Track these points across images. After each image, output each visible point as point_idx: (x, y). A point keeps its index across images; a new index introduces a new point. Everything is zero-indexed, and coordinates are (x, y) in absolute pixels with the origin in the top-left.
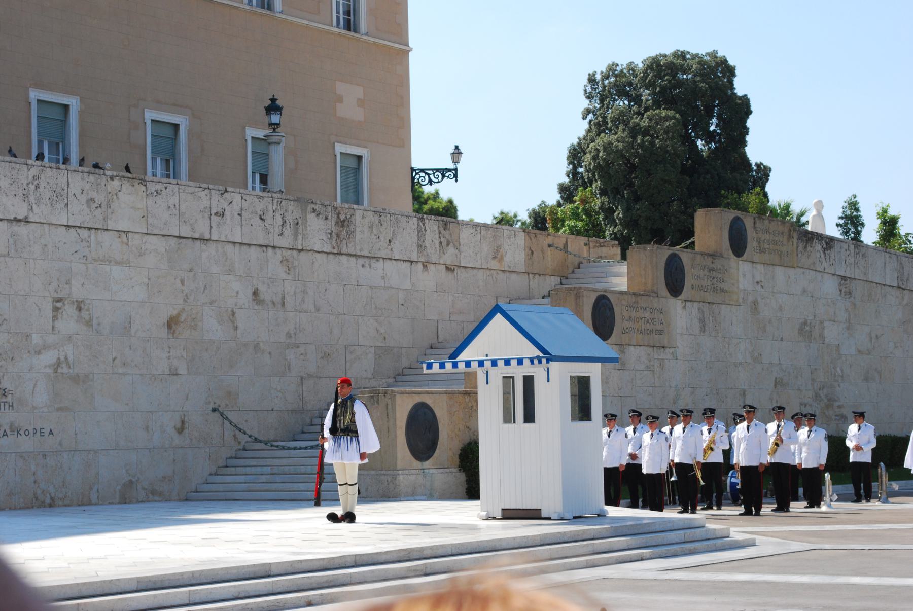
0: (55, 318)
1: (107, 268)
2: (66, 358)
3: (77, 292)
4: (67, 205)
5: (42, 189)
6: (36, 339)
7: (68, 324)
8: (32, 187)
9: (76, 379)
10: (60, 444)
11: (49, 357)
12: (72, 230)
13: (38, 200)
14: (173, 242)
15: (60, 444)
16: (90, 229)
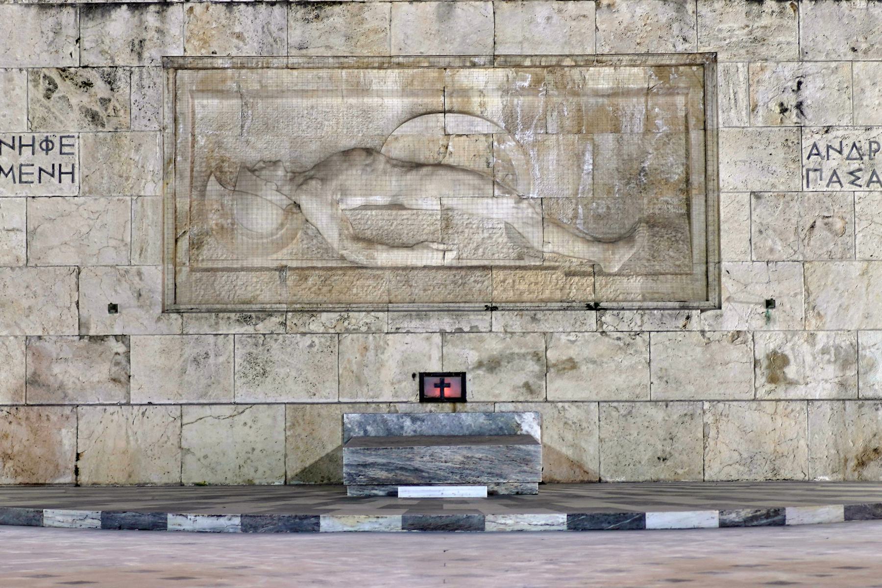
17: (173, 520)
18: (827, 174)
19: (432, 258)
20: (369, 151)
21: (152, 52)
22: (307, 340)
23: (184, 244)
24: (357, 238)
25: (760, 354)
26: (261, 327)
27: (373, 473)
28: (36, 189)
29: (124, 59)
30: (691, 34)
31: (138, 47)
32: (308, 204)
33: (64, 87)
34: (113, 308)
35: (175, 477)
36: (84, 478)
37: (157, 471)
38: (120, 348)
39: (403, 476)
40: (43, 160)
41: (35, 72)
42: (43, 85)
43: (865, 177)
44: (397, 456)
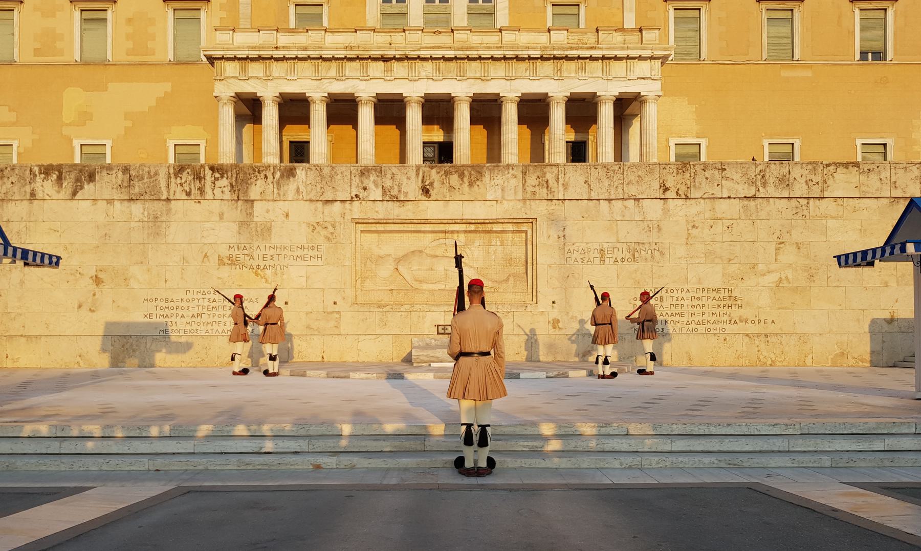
0: (777, 254)
1: (824, 221)
2: (787, 278)
3: (796, 236)
4: (788, 185)
5: (767, 177)
6: (761, 267)
7: (789, 256)
8: (759, 177)
9: (795, 290)
10: (781, 329)
11: (774, 277)
12: (794, 200)
13: (764, 185)
14: (886, 201)
15: (781, 329)
16: (808, 198)
17: (352, 375)
18: (573, 259)
19: (441, 287)
20: (420, 252)
21: (348, 217)
22: (400, 314)
23: (359, 281)
24: (416, 280)
25: (550, 319)
26: (385, 309)
27: (422, 358)
28: (309, 263)
29: (339, 219)
30: (528, 212)
31: (343, 215)
32: (400, 268)
33: (318, 229)
34: (335, 303)
35: (355, 360)
36: (325, 360)
37: (350, 358)
38: (337, 316)
39: (432, 359)
40: (311, 253)
41: (308, 224)
42: (312, 228)
43: (586, 260)
44: (430, 353)
